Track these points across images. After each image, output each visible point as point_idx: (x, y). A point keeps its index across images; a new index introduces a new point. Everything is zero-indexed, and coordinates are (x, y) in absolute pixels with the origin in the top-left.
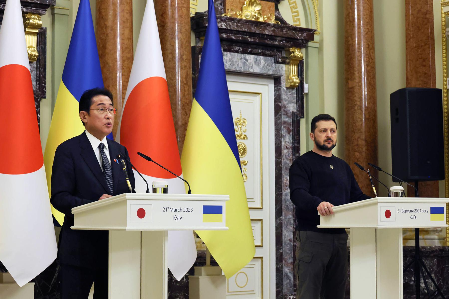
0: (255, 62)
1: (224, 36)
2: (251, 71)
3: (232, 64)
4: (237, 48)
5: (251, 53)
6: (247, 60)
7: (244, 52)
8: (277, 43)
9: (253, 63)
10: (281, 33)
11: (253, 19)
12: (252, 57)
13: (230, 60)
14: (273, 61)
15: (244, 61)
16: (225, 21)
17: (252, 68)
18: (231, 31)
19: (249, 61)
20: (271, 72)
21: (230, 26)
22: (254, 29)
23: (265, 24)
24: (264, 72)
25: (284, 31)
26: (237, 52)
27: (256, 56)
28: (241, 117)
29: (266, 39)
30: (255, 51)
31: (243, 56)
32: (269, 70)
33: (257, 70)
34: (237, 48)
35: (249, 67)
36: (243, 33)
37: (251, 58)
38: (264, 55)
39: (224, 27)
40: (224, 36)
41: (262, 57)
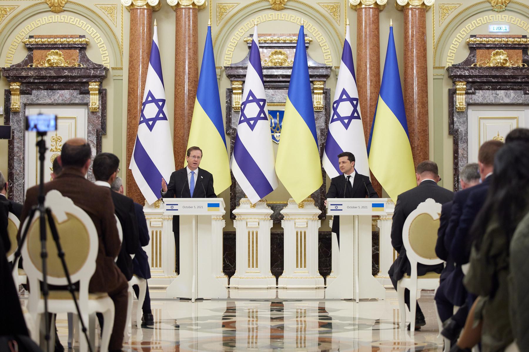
0: (506, 96)
1: (470, 80)
2: (502, 102)
3: (484, 98)
4: (487, 87)
5: (500, 89)
6: (498, 95)
7: (494, 89)
8: (519, 80)
9: (504, 96)
10: (520, 73)
11: (500, 65)
12: (502, 91)
13: (482, 96)
14: (523, 93)
15: (494, 95)
16: (468, 70)
17: (502, 99)
18: (476, 76)
19: (500, 95)
20: (521, 102)
21: (472, 73)
22: (494, 73)
23: (508, 68)
24: (514, 102)
25: (524, 71)
26: (488, 89)
27: (506, 91)
28: (498, 135)
29: (509, 78)
30: (503, 87)
31: (494, 92)
32: (518, 100)
33: (507, 101)
34: (487, 87)
35: (500, 99)
36: (486, 76)
37: (501, 93)
38: (513, 89)
39: (467, 74)
40: (470, 80)
41: (512, 91)
